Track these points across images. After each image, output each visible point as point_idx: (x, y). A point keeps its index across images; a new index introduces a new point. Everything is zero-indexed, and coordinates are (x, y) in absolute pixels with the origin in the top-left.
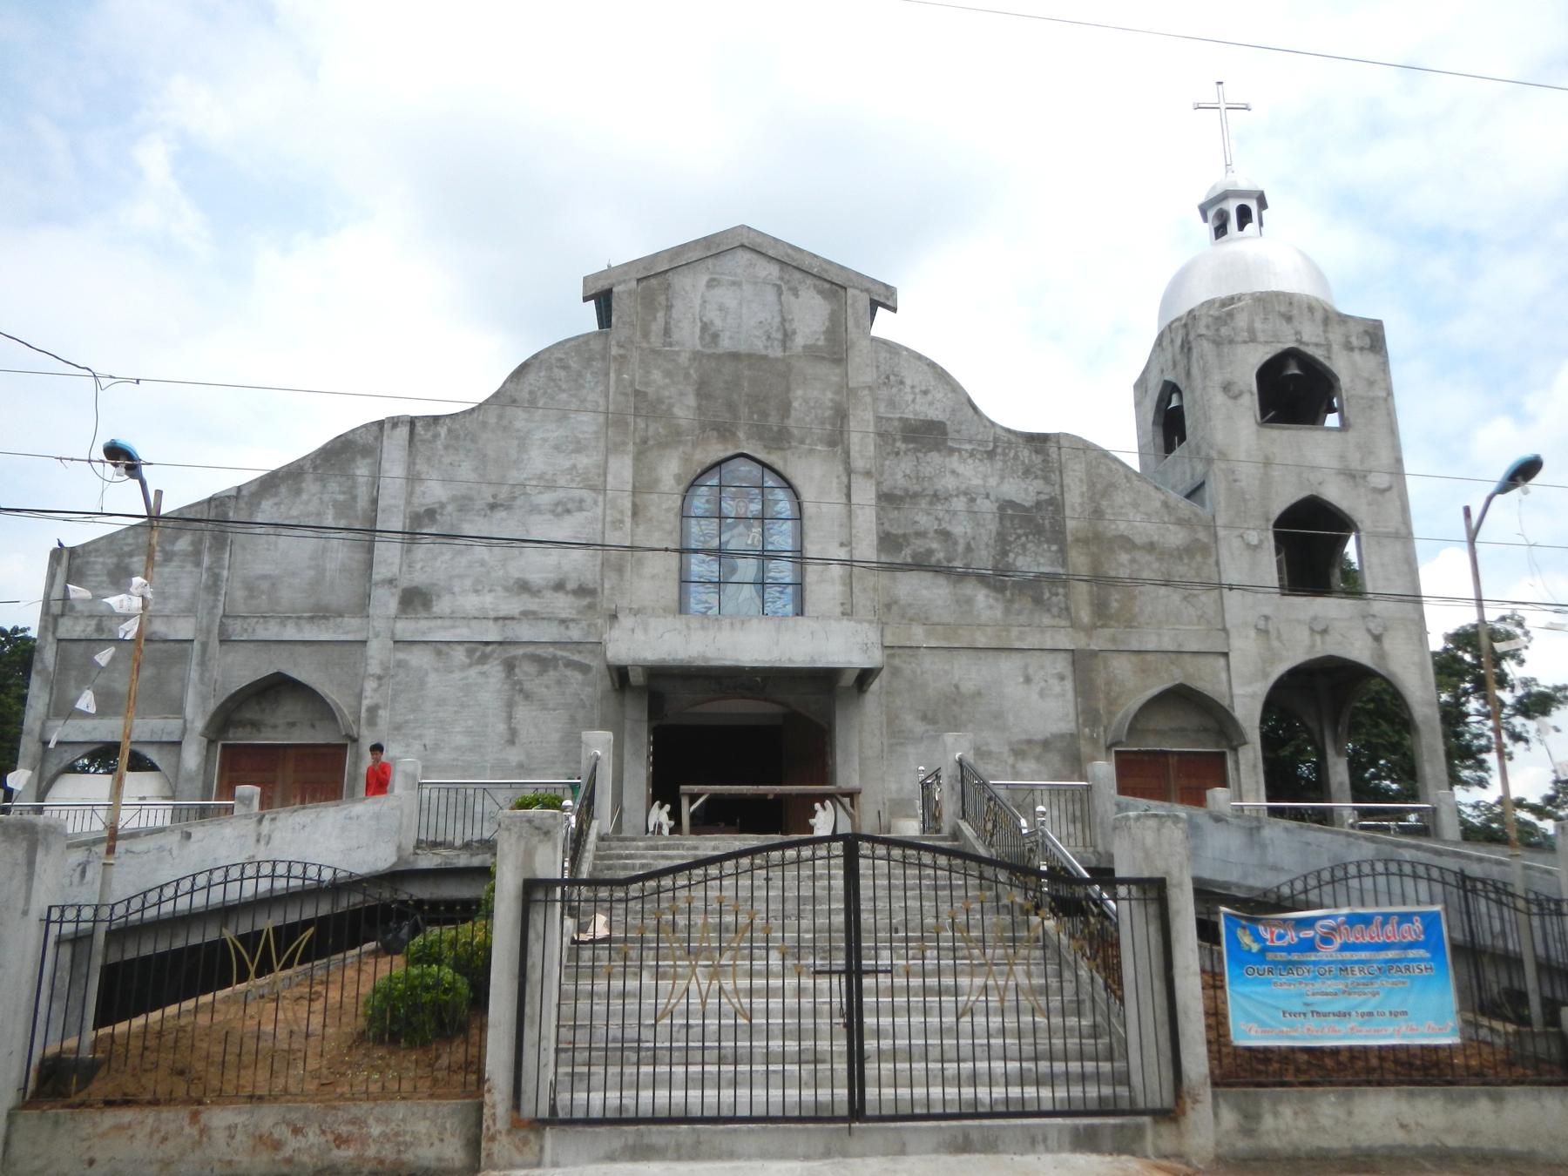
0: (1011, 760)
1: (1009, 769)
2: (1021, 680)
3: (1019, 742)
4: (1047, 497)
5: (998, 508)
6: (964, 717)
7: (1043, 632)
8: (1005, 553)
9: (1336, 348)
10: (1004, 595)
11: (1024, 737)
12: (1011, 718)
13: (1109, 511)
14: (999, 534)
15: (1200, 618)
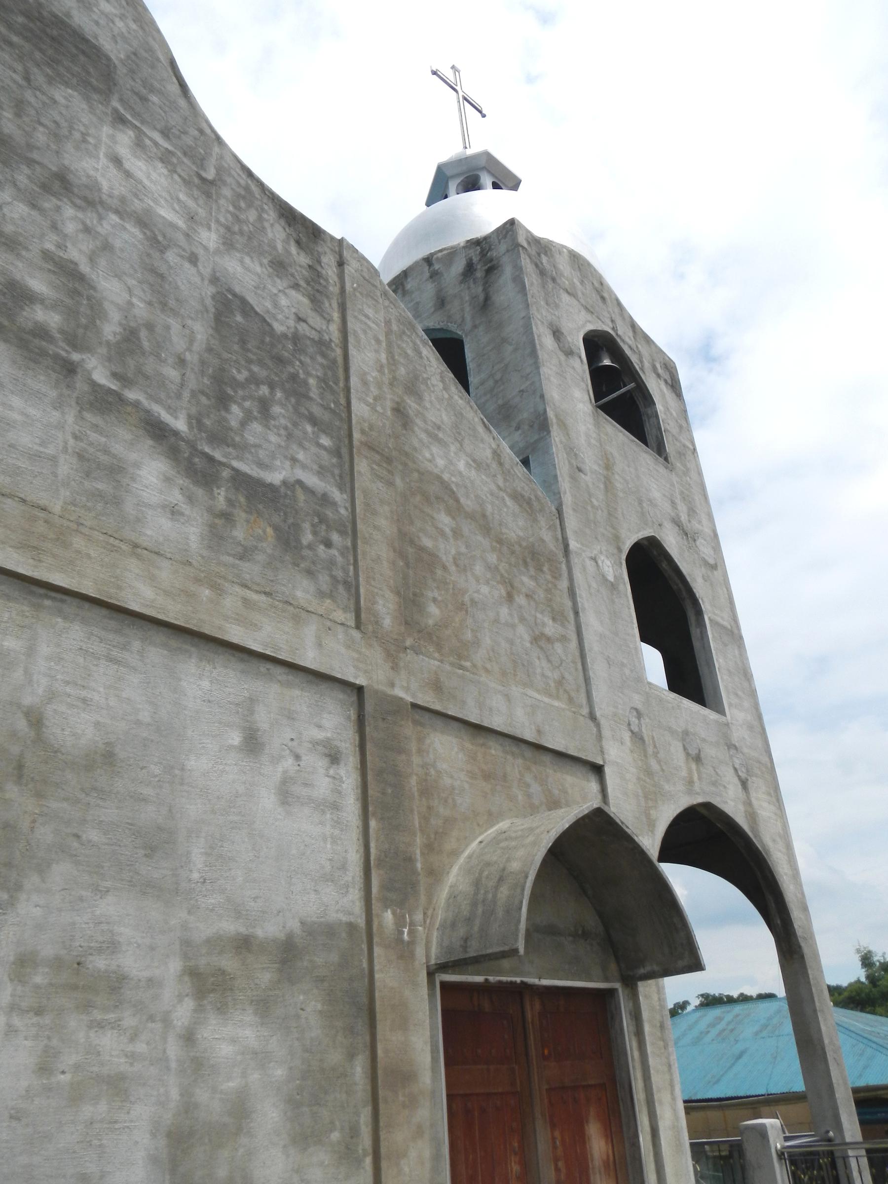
0: (183, 1014)
1: (173, 1049)
2: (235, 738)
3: (216, 943)
4: (314, 335)
5: (213, 297)
6: (45, 834)
7: (296, 620)
8: (223, 401)
9: (647, 365)
10: (213, 498)
11: (230, 927)
12: (198, 858)
13: (419, 421)
14: (210, 350)
15: (560, 683)
